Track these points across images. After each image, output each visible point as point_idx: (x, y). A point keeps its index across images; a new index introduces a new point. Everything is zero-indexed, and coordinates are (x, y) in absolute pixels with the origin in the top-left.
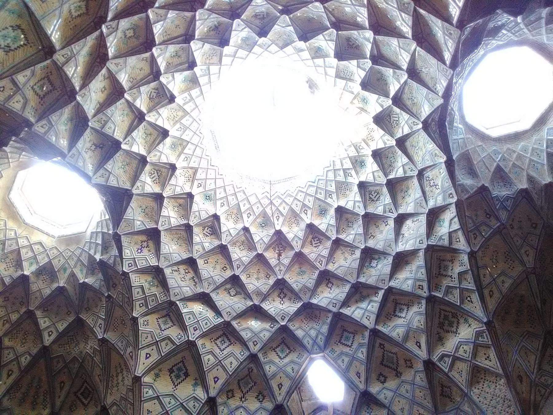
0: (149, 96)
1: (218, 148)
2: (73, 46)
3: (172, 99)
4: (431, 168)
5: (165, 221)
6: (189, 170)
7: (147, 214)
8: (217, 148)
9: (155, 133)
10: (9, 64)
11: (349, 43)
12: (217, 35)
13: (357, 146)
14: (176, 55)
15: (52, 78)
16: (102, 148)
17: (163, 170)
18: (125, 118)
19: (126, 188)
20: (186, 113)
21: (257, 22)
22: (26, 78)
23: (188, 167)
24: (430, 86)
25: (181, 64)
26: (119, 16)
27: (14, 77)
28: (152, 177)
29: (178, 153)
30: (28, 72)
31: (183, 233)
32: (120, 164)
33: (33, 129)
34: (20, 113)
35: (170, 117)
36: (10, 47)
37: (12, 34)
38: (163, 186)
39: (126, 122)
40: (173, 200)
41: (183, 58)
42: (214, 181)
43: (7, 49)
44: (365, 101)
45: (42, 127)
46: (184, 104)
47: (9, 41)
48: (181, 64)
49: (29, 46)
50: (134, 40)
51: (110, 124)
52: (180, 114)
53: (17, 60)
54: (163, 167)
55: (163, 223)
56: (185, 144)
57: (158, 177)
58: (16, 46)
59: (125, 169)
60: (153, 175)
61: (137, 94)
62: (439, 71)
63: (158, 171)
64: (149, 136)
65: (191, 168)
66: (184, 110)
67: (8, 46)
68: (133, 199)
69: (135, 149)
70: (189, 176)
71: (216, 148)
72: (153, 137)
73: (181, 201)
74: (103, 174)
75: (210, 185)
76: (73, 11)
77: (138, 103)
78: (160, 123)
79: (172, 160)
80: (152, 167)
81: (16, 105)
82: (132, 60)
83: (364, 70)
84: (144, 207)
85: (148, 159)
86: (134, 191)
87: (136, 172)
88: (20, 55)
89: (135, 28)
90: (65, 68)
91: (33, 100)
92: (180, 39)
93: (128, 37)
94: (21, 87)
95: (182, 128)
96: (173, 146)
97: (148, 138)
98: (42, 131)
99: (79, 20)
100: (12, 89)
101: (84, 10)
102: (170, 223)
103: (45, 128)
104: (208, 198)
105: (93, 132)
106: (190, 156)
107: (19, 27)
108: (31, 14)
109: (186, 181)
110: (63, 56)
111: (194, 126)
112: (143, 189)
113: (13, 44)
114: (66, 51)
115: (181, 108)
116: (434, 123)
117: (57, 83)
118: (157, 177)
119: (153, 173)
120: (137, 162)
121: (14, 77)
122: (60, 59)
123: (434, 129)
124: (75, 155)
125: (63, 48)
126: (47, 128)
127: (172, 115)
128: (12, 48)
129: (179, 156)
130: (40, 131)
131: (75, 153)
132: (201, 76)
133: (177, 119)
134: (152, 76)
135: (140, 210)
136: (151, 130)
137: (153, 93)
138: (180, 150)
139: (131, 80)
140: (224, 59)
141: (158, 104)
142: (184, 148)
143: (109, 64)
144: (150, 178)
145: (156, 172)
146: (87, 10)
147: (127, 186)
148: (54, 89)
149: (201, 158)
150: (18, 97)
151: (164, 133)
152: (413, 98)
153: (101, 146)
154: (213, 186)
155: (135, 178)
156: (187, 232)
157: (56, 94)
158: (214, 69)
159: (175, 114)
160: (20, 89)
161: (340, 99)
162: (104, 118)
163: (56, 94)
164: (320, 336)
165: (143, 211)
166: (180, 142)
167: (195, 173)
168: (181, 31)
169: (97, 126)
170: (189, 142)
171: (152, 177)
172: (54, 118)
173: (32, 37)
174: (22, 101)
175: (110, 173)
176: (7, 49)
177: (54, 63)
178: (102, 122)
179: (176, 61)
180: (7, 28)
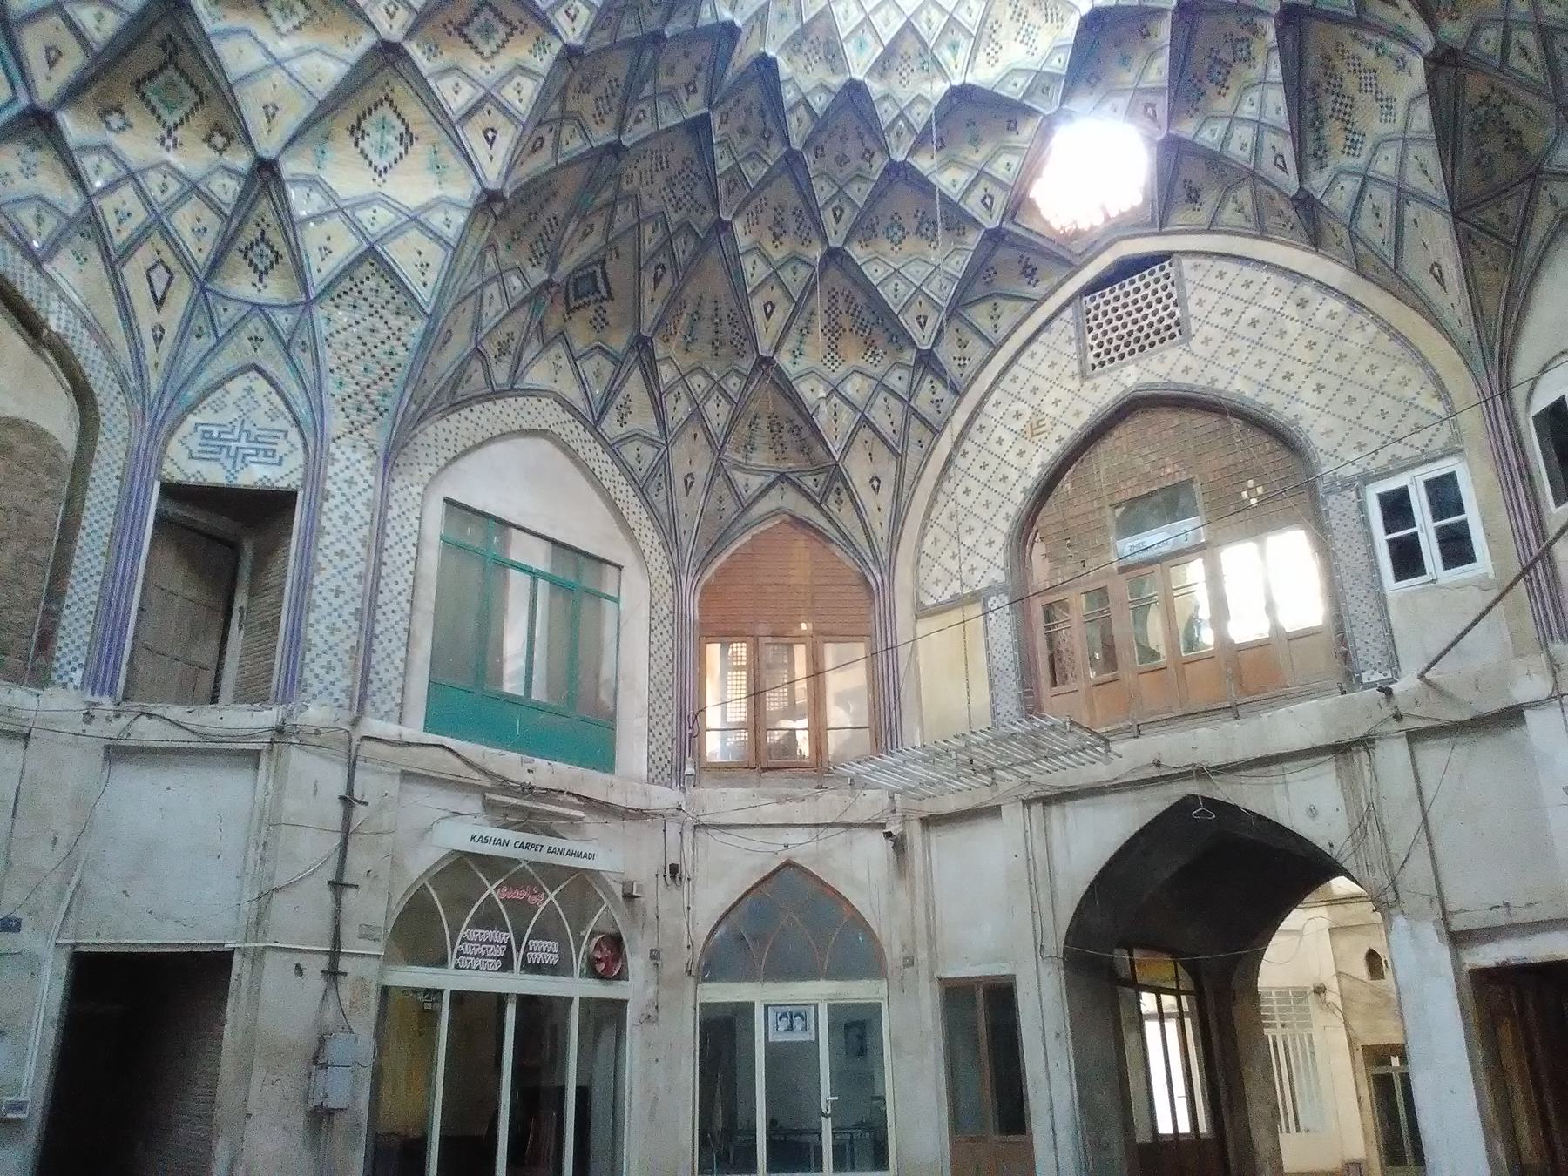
10: (434, 132)
22: (461, 83)
30: (444, 88)
33: (580, 42)
34: (542, 81)
36: (401, 135)
37: (375, 135)
43: (407, 139)
47: (390, 139)
49: (391, 96)
53: (424, 115)
58: (398, 123)
81: (522, 95)
88: (414, 112)
91: (518, 51)
94: (482, 92)
100: (489, 112)
108: (310, 123)
110: (392, 16)
113: (393, 127)
121: (455, 118)
128: (403, 129)
150: (509, 94)
173: (371, 94)
174: (518, 79)
176: (407, 139)
177: (410, 33)
180: (362, 152)
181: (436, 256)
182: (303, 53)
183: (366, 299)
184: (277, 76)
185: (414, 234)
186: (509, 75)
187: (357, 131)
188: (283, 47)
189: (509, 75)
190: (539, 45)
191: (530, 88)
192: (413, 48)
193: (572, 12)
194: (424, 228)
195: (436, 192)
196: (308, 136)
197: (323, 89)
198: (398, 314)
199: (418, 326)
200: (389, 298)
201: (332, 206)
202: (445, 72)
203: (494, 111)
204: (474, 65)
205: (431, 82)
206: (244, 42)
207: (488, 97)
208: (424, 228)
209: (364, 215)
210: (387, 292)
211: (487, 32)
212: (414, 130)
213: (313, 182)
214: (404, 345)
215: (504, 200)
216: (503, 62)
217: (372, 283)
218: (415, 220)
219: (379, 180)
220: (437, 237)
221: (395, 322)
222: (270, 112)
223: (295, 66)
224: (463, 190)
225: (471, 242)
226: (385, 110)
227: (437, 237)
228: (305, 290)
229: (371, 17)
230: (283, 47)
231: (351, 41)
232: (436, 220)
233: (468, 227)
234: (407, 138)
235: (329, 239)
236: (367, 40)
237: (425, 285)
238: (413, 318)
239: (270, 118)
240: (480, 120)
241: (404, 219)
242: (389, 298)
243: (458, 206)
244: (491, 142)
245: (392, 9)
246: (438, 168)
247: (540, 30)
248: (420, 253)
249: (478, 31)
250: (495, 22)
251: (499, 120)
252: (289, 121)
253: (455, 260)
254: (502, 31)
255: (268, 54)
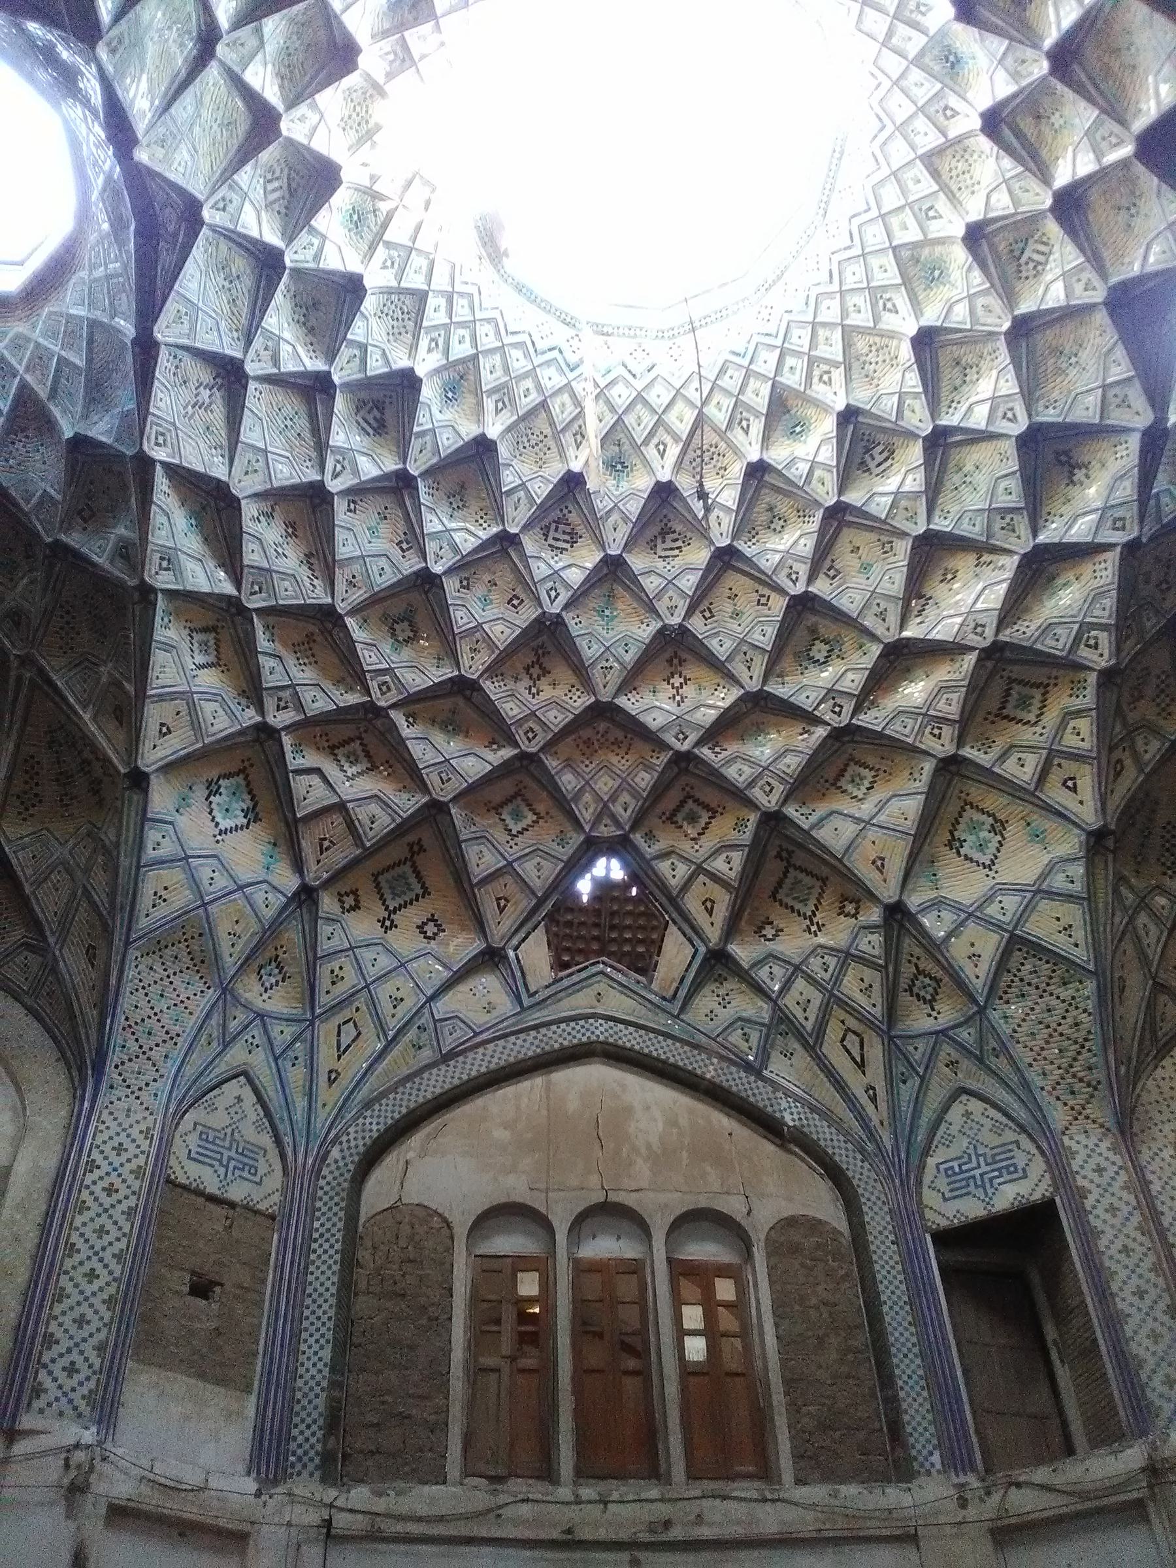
0: (890, 462)
1: (838, 149)
2: (910, 740)
3: (848, 416)
4: (175, 85)
5: (1104, 139)
6: (945, 176)
7: (1133, 193)
8: (839, 154)
9: (945, 357)
10: (1019, 808)
11: (378, 415)
12: (671, 516)
13: (403, 60)
14: (775, 522)
15: (994, 705)
16: (1066, 453)
17: (1002, 247)
18: (969, 467)
19: (1108, 321)
20: (848, 334)
21: (574, 517)
23: (944, 188)
24: (187, 359)
25: (777, 490)
26: (810, 719)
27: (1032, 787)
28: (1041, 258)
29: (938, 249)
31: (1091, 53)
32: (1073, 372)
33: (1113, 662)
34: (1094, 713)
35: (887, 358)
37: (971, 839)
38: (1034, 219)
39: (975, 456)
40: (1044, 153)
41: (768, 497)
42: (904, 83)
43: (998, 826)
44: (355, 217)
45: (1096, 647)
46: (836, 365)
47: (984, 834)
48: (777, 490)
49: (969, 799)
50: (822, 631)
51: (1004, 501)
52: (861, 344)
53: (1004, 800)
54: (997, 257)
55: (1114, 140)
56: (905, 254)
57: (1031, 241)
59: (1074, 351)
60: (1036, 257)
61: (903, 503)
62: (174, 424)
63: (1017, 253)
64: (963, 362)
65: (935, 174)
66: (847, 345)
67: (993, 829)
68: (1122, 277)
69: (1009, 385)
70: (958, 157)
71: (842, 153)
72: (957, 351)
73: (1026, 124)
74: (1118, 406)
75: (924, 87)
76: (866, 784)
77: (915, 482)
78: (913, 381)
79: (959, 255)
80: (1019, 286)
82: (850, 602)
83: (352, 343)
84: (1123, 216)
85: (1006, 325)
86: (1098, 295)
87: (1060, 319)
88: (994, 801)
89: (806, 659)
90: (956, 717)
91: (1061, 701)
92: (739, 565)
93: (827, 647)
94: (1045, 752)
95: (881, 302)
96: (937, 273)
97: (969, 359)
98: (1103, 637)
99: (871, 761)
100: (1059, 765)
101: (853, 769)
102: (1097, 124)
103: (1096, 638)
104: (952, 58)
105: (1045, 517)
106: (916, 208)
107: (950, 845)
108: (913, 859)
109: (975, 156)
111: (854, 275)
112: (1079, 269)
114: (929, 743)
115: (849, 363)
116: (171, 229)
117: (997, 688)
118: (1032, 245)
119: (1031, 265)
120: (1038, 337)
122: (949, 737)
123: (168, 210)
124: (1115, 521)
125: (926, 753)
126: (1093, 633)
127: (880, 359)
129: (941, 241)
130: (1106, 642)
131: (1109, 523)
132: (757, 414)
133: (877, 339)
134: (848, 518)
135: (1137, 222)
136: (948, 375)
137: (879, 459)
138: (926, 252)
139: (887, 547)
140: (683, 429)
141: (884, 430)
142: (916, 245)
143: (890, 637)
144: (1047, 261)
145: (1023, 260)
146: (847, 765)
147: (1101, 317)
148: (1011, 681)
149: (882, 216)
150: (1070, 741)
151: (927, 340)
152: (227, 284)
153: (1063, 458)
154: (916, 75)
155: (1071, 314)
156: (1079, 46)
157: (1017, 671)
158: (718, 415)
159: (872, 357)
160: (1051, 750)
161: (426, 209)
162: (998, 524)
163: (1017, 671)
164: (625, 797)
165: (1133, 211)
166: (912, 271)
167: (939, 152)
168: (734, 581)
169: (1022, 525)
170: (894, 249)
171: (1041, 258)
172: (1058, 644)
173: (952, 808)
174: (1072, 724)
175: (1105, 387)
176: (998, 826)
177: (960, 742)
178: (1008, 520)
179: (784, 506)
181: (1074, 914)
182: (881, 806)
183: (1029, 984)
184: (872, 833)
185: (1044, 905)
186: (1062, 725)
187: (954, 843)
188: (866, 809)
189: (1062, 725)
190: (1077, 686)
191: (1084, 725)
192: (968, 752)
193: (1092, 642)
194: (1052, 895)
195: (1046, 859)
196: (917, 867)
197: (910, 826)
198: (1065, 984)
199: (1090, 987)
200: (1049, 972)
201: (963, 916)
202: (1003, 757)
203: (1063, 762)
204: (1027, 735)
205: (996, 770)
206: (837, 821)
207: (1052, 754)
208: (1052, 895)
209: (992, 910)
210: (1045, 968)
211: (1024, 703)
212: (1001, 816)
213: (937, 904)
214: (1085, 1011)
215: (1113, 833)
216: (1051, 717)
217: (1029, 966)
218: (1040, 892)
219: (992, 874)
220: (1068, 897)
221: (1066, 994)
222: (879, 864)
223: (882, 818)
224: (1069, 844)
225: (1101, 883)
226: (970, 813)
227: (1068, 897)
228: (975, 1002)
229: (923, 747)
230: (866, 809)
231: (916, 776)
232: (1058, 882)
233: (1090, 873)
234: (999, 826)
235: (973, 945)
236: (928, 766)
237: (1077, 945)
238: (1081, 982)
239: (880, 870)
240: (1055, 777)
241: (1029, 895)
242: (1049, 972)
243: (1072, 860)
244: (1074, 789)
245: (936, 731)
246: (1037, 837)
247: (1071, 674)
248: (1058, 919)
249: (1016, 707)
250: (1026, 691)
251: (1070, 767)
252: (896, 865)
253: (1093, 911)
254: (1037, 694)
255: (858, 820)
